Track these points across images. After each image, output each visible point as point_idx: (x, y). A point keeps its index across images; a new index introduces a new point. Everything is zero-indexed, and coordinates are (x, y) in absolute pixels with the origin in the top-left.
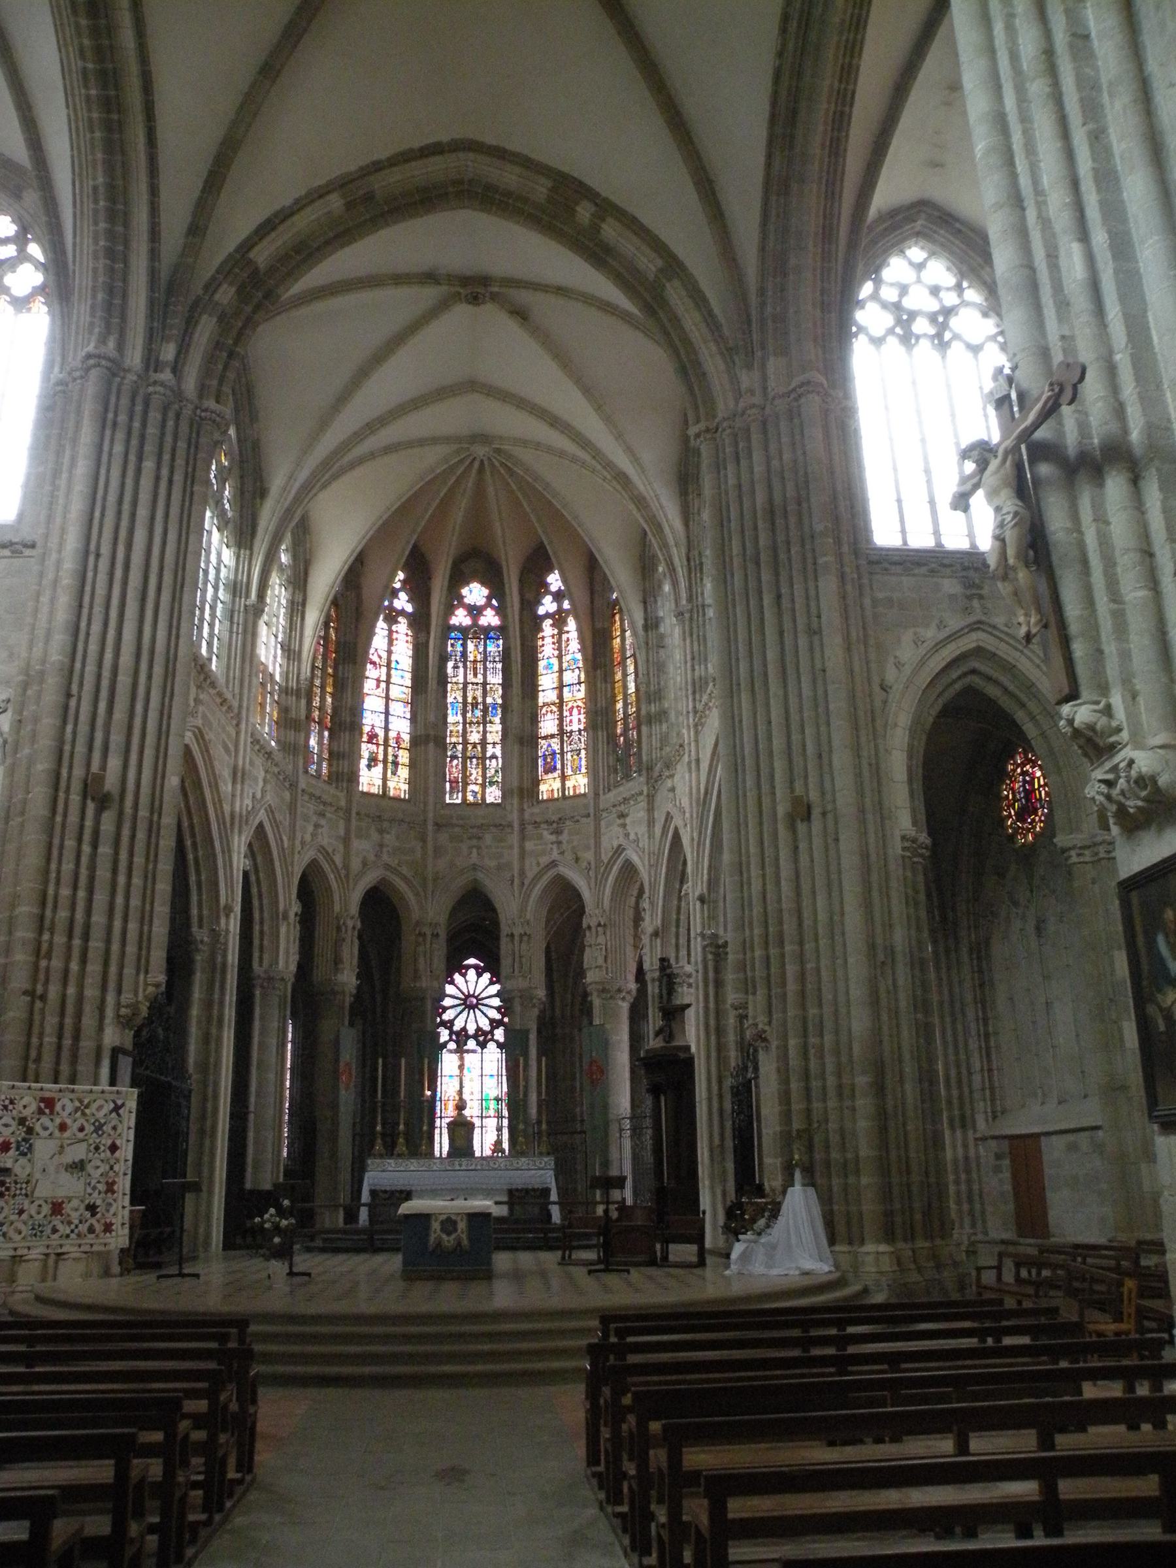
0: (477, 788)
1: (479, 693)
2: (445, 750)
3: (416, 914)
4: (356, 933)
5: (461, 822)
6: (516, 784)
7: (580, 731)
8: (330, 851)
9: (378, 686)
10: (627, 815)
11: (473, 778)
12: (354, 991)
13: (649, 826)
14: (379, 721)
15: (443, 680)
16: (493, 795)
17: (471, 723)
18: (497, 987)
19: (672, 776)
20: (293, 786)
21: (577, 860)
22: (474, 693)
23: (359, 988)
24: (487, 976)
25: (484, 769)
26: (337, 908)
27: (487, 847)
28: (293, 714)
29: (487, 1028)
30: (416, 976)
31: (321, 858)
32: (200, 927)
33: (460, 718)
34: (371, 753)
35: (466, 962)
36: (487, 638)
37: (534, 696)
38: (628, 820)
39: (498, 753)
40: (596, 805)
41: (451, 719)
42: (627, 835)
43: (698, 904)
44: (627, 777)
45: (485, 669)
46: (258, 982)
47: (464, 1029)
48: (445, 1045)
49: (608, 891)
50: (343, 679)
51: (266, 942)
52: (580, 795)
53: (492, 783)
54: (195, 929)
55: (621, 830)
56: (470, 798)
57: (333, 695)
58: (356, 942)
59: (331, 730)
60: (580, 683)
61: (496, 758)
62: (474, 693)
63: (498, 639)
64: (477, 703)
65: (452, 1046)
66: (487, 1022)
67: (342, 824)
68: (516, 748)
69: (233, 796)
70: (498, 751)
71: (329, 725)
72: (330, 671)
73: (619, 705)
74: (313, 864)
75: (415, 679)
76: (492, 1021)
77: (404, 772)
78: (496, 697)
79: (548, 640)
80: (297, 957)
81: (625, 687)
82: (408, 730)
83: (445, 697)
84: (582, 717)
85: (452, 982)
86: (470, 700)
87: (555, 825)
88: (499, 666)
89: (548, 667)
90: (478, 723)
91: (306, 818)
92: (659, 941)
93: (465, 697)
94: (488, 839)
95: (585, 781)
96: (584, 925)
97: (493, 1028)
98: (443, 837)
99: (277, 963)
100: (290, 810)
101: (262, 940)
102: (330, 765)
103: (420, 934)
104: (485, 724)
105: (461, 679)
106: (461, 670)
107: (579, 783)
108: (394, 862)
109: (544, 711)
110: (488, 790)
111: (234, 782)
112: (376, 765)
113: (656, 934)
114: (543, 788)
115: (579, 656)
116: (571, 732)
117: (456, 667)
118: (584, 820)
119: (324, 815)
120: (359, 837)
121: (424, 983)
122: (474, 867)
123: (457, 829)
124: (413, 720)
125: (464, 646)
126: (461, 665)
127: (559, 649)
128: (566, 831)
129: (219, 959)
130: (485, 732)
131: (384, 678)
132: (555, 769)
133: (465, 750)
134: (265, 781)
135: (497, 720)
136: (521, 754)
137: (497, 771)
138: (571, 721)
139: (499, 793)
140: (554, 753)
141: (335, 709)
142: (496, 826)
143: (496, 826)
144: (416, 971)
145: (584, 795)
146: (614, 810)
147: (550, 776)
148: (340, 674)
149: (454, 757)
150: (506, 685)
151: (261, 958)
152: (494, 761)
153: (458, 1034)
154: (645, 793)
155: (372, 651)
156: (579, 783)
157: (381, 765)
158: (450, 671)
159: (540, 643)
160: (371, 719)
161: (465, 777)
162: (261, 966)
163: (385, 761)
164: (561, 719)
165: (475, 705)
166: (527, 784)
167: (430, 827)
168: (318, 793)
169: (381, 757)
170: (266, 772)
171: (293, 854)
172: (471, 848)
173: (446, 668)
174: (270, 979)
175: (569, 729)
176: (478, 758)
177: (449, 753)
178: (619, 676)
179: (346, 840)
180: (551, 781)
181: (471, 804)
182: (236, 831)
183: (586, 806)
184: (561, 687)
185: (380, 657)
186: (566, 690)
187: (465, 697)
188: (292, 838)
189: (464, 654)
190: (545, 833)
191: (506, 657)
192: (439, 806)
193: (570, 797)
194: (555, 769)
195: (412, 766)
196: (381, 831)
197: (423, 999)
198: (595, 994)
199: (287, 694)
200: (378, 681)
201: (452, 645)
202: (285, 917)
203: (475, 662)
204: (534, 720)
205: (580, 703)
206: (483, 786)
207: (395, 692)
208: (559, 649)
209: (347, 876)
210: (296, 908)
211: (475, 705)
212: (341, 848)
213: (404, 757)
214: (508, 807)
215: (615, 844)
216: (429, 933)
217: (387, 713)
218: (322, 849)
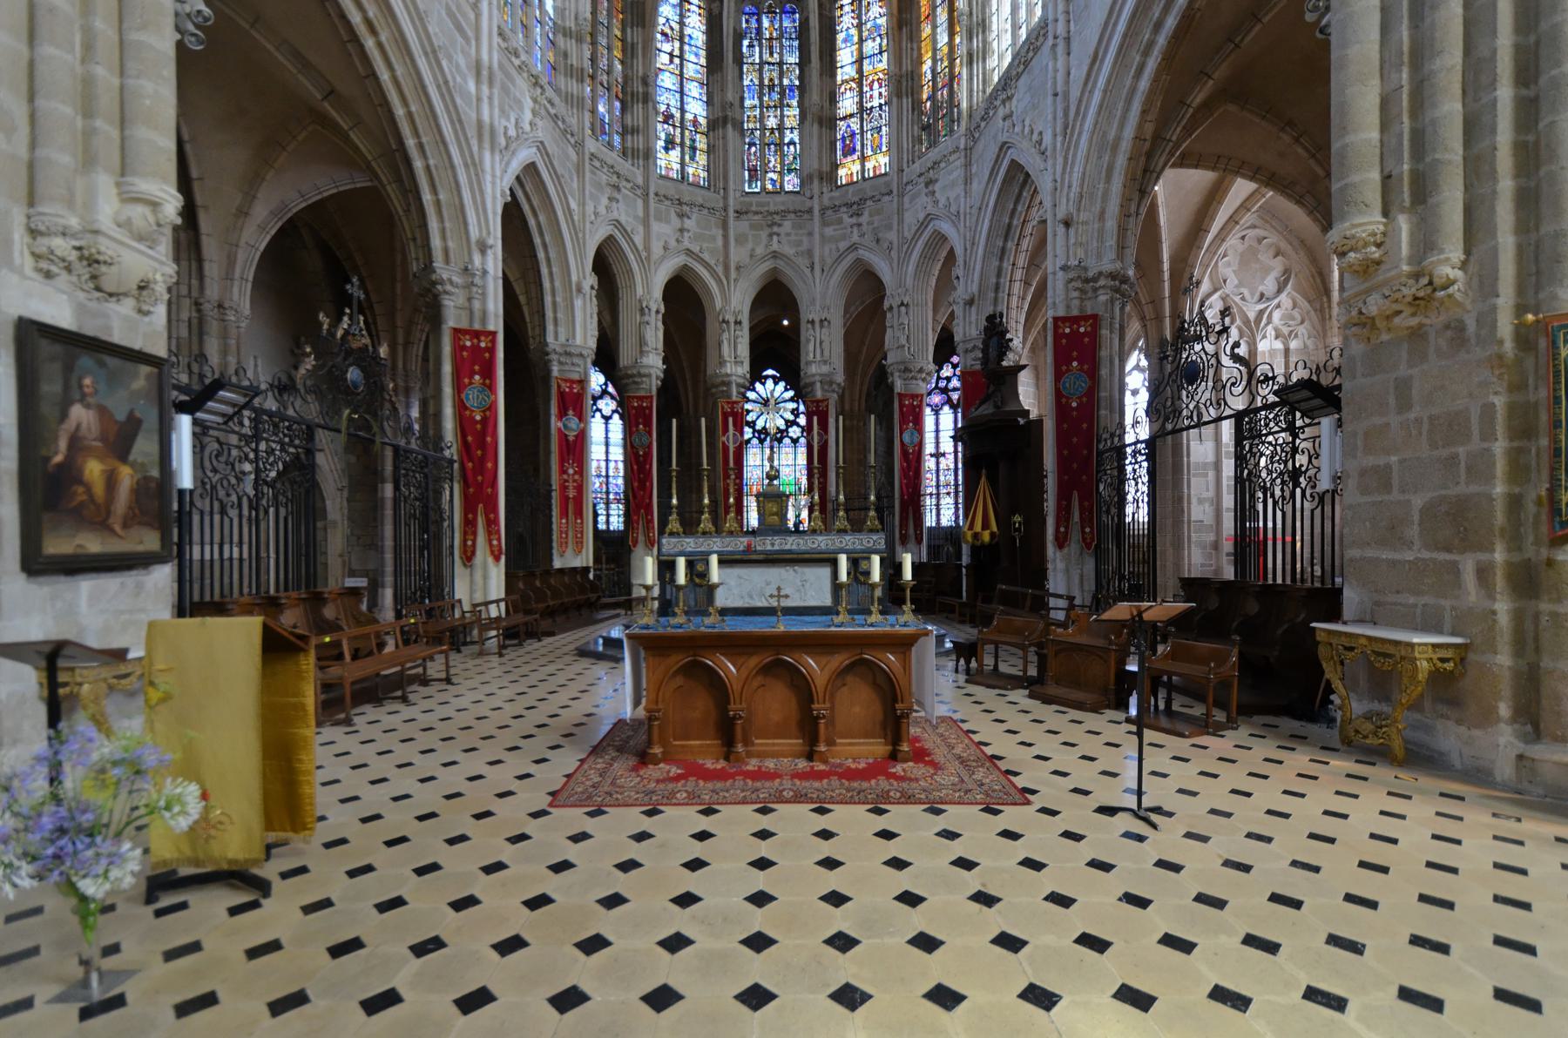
0: (774, 176)
1: (775, 75)
3: (718, 304)
4: (660, 316)
5: (759, 209)
6: (816, 166)
7: (881, 105)
8: (629, 229)
9: (671, 62)
10: (936, 181)
11: (771, 165)
12: (662, 375)
13: (966, 184)
14: (674, 101)
15: (739, 60)
16: (791, 183)
17: (768, 107)
18: (791, 393)
19: (1009, 98)
20: (579, 146)
21: (878, 241)
22: (770, 74)
23: (665, 372)
24: (782, 385)
25: (783, 156)
26: (640, 291)
27: (788, 234)
28: (574, 60)
29: (783, 427)
30: (722, 363)
31: (619, 236)
32: (447, 261)
33: (756, 102)
34: (668, 135)
35: (765, 373)
36: (784, 12)
37: (834, 75)
38: (937, 187)
39: (797, 140)
40: (900, 178)
41: (748, 103)
42: (936, 202)
43: (1061, 229)
44: (933, 144)
45: (782, 46)
46: (554, 357)
47: (764, 428)
48: (748, 441)
49: (911, 268)
50: (633, 44)
51: (560, 315)
52: (881, 175)
53: (790, 171)
54: (438, 263)
55: (929, 199)
56: (769, 187)
57: (622, 62)
58: (660, 325)
59: (623, 103)
60: (881, 53)
61: (794, 144)
62: (770, 74)
63: (794, 13)
64: (774, 85)
65: (755, 441)
66: (783, 422)
67: (640, 203)
68: (816, 126)
69: (479, 99)
70: (796, 137)
71: (620, 95)
72: (619, 34)
73: (927, 67)
74: (610, 239)
75: (708, 58)
76: (787, 422)
77: (702, 159)
78: (791, 79)
79: (847, 9)
80: (596, 333)
81: (935, 42)
82: (704, 114)
83: (741, 79)
84: (883, 90)
85: (754, 390)
86: (766, 82)
87: (855, 207)
88: (796, 43)
89: (845, 41)
90: (775, 107)
91: (598, 186)
92: (974, 309)
93: (761, 79)
94: (787, 225)
95: (887, 159)
96: (886, 305)
97: (788, 427)
98: (744, 226)
99: (574, 337)
100: (578, 173)
101: (555, 311)
102: (623, 140)
103: (724, 321)
104: (782, 106)
105: (757, 61)
106: (757, 49)
107: (880, 162)
108: (696, 249)
109: (842, 90)
110: (786, 179)
111: (478, 82)
112: (673, 148)
113: (970, 303)
114: (842, 172)
115: (882, 21)
116: (872, 108)
117: (751, 46)
118: (887, 198)
119: (617, 188)
120: (659, 219)
121: (729, 369)
122: (775, 255)
123: (756, 217)
124: (709, 103)
125: (759, 21)
126: (756, 43)
127: (859, 17)
128: (866, 213)
129: (477, 305)
130: (782, 116)
131: (677, 52)
132: (854, 150)
133: (763, 135)
134: (534, 113)
135: (794, 103)
136: (820, 137)
137: (795, 158)
138: (871, 96)
139: (797, 181)
140: (853, 134)
141: (625, 77)
142: (795, 212)
143: (795, 212)
144: (720, 356)
145: (886, 174)
146: (922, 179)
147: (849, 159)
148: (629, 40)
149: (751, 144)
150: (803, 63)
151: (556, 333)
152: (792, 147)
153: (760, 432)
154: (962, 146)
155: (661, 20)
156: (880, 162)
157: (678, 149)
158: (744, 50)
159: (838, 13)
160: (666, 100)
161: (765, 164)
162: (556, 338)
163: (682, 144)
164: (861, 93)
165: (771, 87)
166: (826, 168)
167: (731, 214)
168: (610, 162)
169: (678, 140)
170: (535, 101)
171: (584, 222)
172: (771, 235)
173: (741, 46)
174: (568, 354)
175: (869, 105)
176: (776, 145)
177: (747, 140)
178: (927, 30)
179: (646, 222)
180: (850, 165)
181: (769, 193)
182: (487, 145)
183: (888, 184)
184: (860, 61)
185: (672, 29)
186: (866, 62)
187: (761, 79)
188: (583, 204)
189: (759, 31)
190: (845, 217)
191: (803, 33)
192: (738, 194)
193: (870, 178)
194: (854, 150)
195: (710, 150)
196: (681, 216)
197: (728, 384)
198: (896, 374)
199: (565, 35)
200: (671, 55)
201: (747, 21)
202: (579, 290)
203: (771, 39)
204: (833, 99)
205: (881, 76)
206: (781, 174)
207: (690, 70)
208: (859, 17)
209: (648, 258)
210: (591, 280)
211: (771, 87)
212: (641, 229)
213: (701, 142)
214: (808, 194)
215: (921, 216)
216: (732, 320)
217: (682, 93)
218: (617, 224)
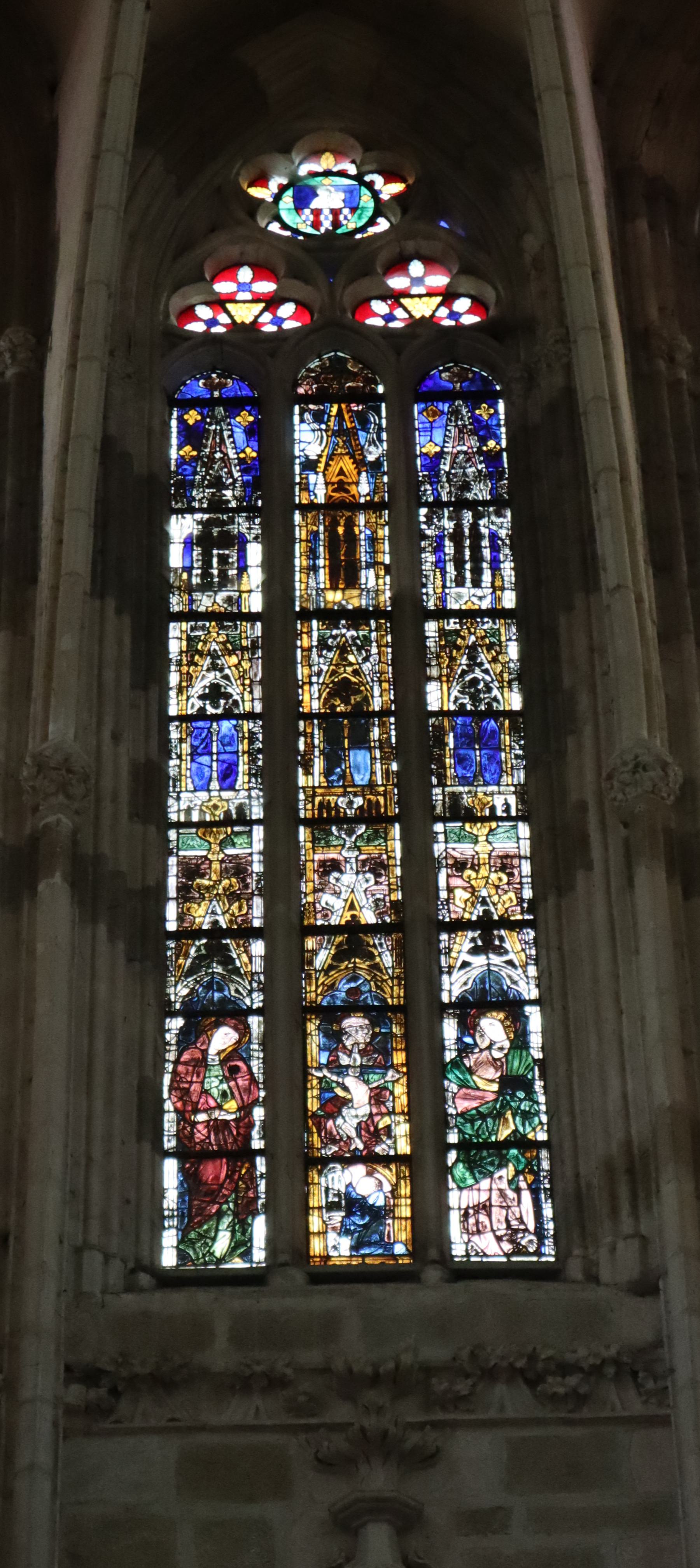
2: (161, 969)
105: (255, 603)
106: (255, 553)
110: (457, 1199)
158: (176, 558)
177: (178, 992)
201: (191, 435)
